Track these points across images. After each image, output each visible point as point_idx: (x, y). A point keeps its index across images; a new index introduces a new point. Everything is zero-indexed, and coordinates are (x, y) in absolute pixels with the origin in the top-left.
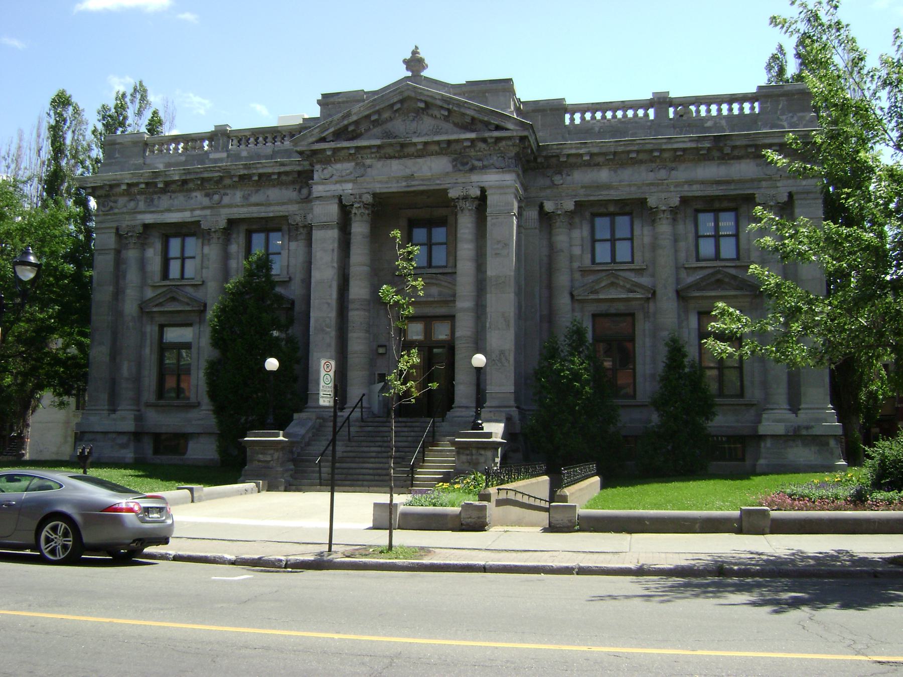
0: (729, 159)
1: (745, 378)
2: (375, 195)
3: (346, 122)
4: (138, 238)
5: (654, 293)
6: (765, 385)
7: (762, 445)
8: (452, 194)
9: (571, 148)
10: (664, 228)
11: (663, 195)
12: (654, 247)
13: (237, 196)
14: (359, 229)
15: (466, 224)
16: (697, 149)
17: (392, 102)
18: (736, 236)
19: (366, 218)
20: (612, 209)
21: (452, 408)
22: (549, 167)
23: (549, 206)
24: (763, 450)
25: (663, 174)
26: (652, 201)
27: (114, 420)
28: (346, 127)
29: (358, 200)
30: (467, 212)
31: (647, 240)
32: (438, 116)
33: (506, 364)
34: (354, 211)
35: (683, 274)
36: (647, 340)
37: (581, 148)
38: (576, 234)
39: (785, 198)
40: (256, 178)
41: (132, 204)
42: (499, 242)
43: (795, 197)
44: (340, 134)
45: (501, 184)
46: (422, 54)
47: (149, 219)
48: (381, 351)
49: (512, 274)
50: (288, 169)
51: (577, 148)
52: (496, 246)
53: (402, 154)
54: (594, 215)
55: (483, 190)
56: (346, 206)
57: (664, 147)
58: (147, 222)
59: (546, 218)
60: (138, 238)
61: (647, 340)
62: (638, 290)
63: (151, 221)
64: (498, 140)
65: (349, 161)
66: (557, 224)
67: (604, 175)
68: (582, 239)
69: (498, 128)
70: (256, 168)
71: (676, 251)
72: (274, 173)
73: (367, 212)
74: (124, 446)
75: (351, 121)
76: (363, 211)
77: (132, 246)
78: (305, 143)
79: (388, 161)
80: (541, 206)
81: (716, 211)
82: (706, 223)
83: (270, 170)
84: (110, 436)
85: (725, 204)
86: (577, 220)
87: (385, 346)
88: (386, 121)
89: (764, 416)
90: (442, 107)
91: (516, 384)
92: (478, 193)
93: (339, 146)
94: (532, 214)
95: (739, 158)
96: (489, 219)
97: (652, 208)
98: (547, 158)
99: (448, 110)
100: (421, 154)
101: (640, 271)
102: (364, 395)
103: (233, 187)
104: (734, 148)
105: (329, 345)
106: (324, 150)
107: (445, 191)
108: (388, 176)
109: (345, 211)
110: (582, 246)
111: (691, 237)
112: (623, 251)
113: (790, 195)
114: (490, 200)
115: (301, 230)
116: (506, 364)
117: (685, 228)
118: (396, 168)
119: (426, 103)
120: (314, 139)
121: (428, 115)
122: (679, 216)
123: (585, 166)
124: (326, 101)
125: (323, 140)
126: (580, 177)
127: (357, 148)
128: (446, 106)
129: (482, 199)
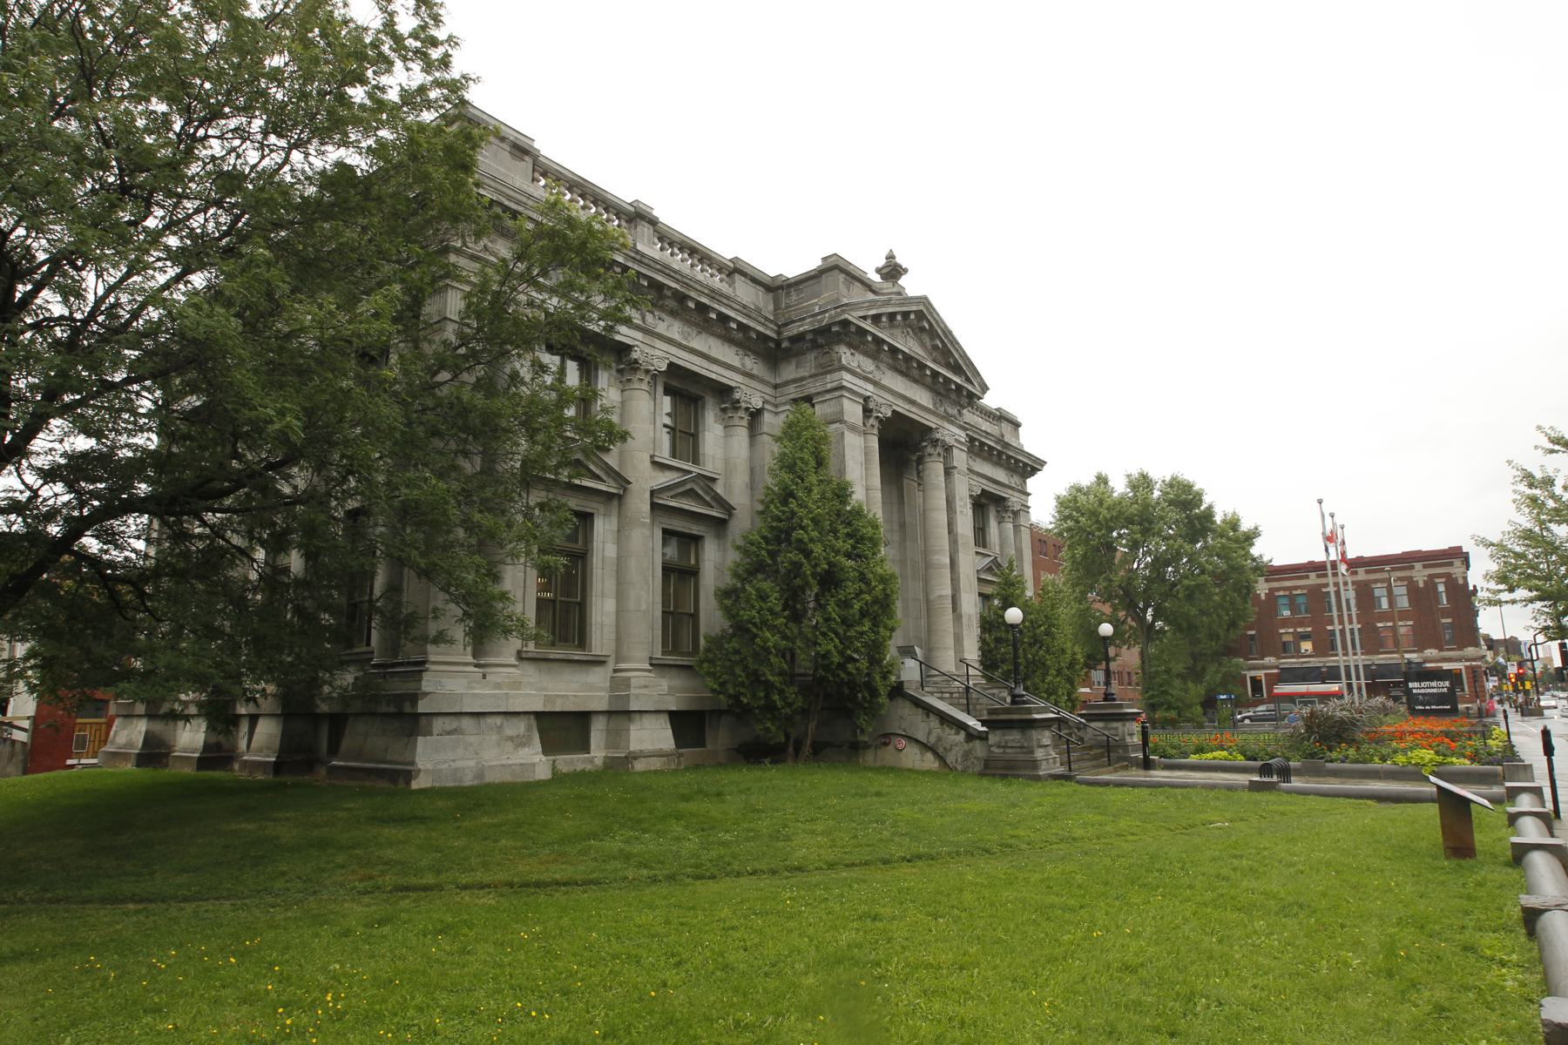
13: (673, 328)
15: (935, 469)
27: (498, 686)
34: (872, 421)
46: (899, 260)
50: (752, 324)
72: (734, 320)
74: (520, 742)
83: (732, 314)
84: (490, 720)
106: (862, 332)
114: (955, 451)
115: (742, 413)
119: (931, 324)
124: (835, 268)
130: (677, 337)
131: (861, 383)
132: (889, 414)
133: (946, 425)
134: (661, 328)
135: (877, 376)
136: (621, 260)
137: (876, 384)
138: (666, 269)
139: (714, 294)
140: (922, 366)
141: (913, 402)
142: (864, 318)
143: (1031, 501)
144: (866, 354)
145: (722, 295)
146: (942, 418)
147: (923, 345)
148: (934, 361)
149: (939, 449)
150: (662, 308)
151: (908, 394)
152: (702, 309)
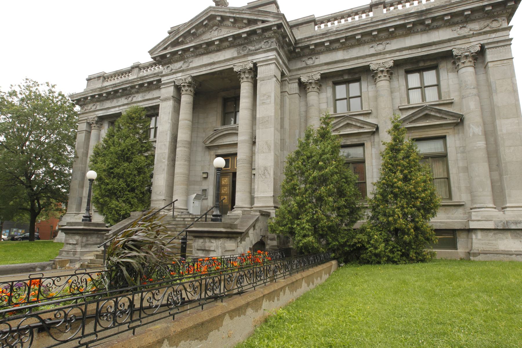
0: (430, 29)
1: (452, 185)
2: (194, 78)
3: (177, 37)
4: (96, 123)
5: (377, 129)
6: (471, 191)
7: (474, 237)
8: (236, 69)
9: (317, 39)
10: (383, 83)
11: (381, 61)
12: (376, 98)
13: (139, 97)
14: (186, 99)
16: (403, 26)
17: (202, 20)
18: (438, 85)
19: (188, 92)
20: (346, 77)
21: (234, 208)
22: (304, 56)
23: (304, 79)
24: (474, 241)
25: (380, 48)
26: (372, 67)
28: (178, 39)
29: (184, 81)
30: (245, 80)
31: (371, 94)
32: (229, 24)
33: (268, 176)
35: (399, 113)
36: (374, 161)
37: (323, 38)
38: (323, 95)
39: (478, 48)
40: (146, 85)
41: (94, 107)
42: (264, 95)
43: (486, 47)
44: (176, 43)
45: (268, 62)
47: (100, 114)
48: (205, 176)
49: (273, 114)
51: (320, 38)
52: (263, 98)
53: (208, 51)
54: (336, 84)
55: (255, 65)
56: (177, 86)
57: (380, 27)
58: (100, 115)
59: (303, 86)
60: (96, 123)
61: (374, 161)
62: (365, 126)
63: (102, 115)
64: (264, 30)
65: (180, 61)
66: (310, 90)
67: (340, 55)
68: (327, 98)
69: (263, 22)
70: (146, 79)
71: (392, 99)
72: (154, 81)
73: (190, 89)
75: (180, 35)
76: (187, 88)
77: (93, 128)
78: (156, 52)
79: (201, 57)
80: (299, 79)
81: (421, 70)
82: (414, 79)
85: (428, 64)
86: (323, 87)
87: (207, 173)
88: (200, 35)
89: (473, 213)
90: (230, 17)
91: (275, 190)
92: (251, 65)
93: (173, 50)
94: (295, 86)
95: (438, 28)
96: (258, 81)
97: (374, 71)
98: (302, 48)
99: (234, 18)
100: (219, 49)
101: (368, 114)
102: (177, 200)
103: (137, 92)
104: (434, 19)
105: (164, 170)
106: (166, 54)
107: (232, 69)
108: (202, 65)
109: (178, 89)
110: (327, 102)
111: (403, 88)
112: (355, 104)
113: (482, 47)
114: (259, 69)
116: (268, 176)
117: (399, 82)
118: (206, 59)
119: (222, 17)
120: (161, 49)
121: (224, 26)
122: (394, 75)
123: (327, 51)
125: (165, 48)
126: (324, 58)
127: (182, 50)
128: (232, 15)
129: (254, 70)
130: (140, 99)
131: (174, 76)
132: (190, 79)
133: (250, 58)
134: (135, 100)
135: (184, 67)
136: (111, 90)
137: (183, 71)
138: (123, 83)
139: (142, 78)
140: (213, 43)
141: (213, 63)
142: (165, 48)
143: (512, 34)
144: (177, 61)
145: (144, 77)
146: (245, 56)
147: (228, 27)
148: (240, 28)
149: (242, 76)
150: (133, 93)
151: (212, 61)
152: (142, 85)
